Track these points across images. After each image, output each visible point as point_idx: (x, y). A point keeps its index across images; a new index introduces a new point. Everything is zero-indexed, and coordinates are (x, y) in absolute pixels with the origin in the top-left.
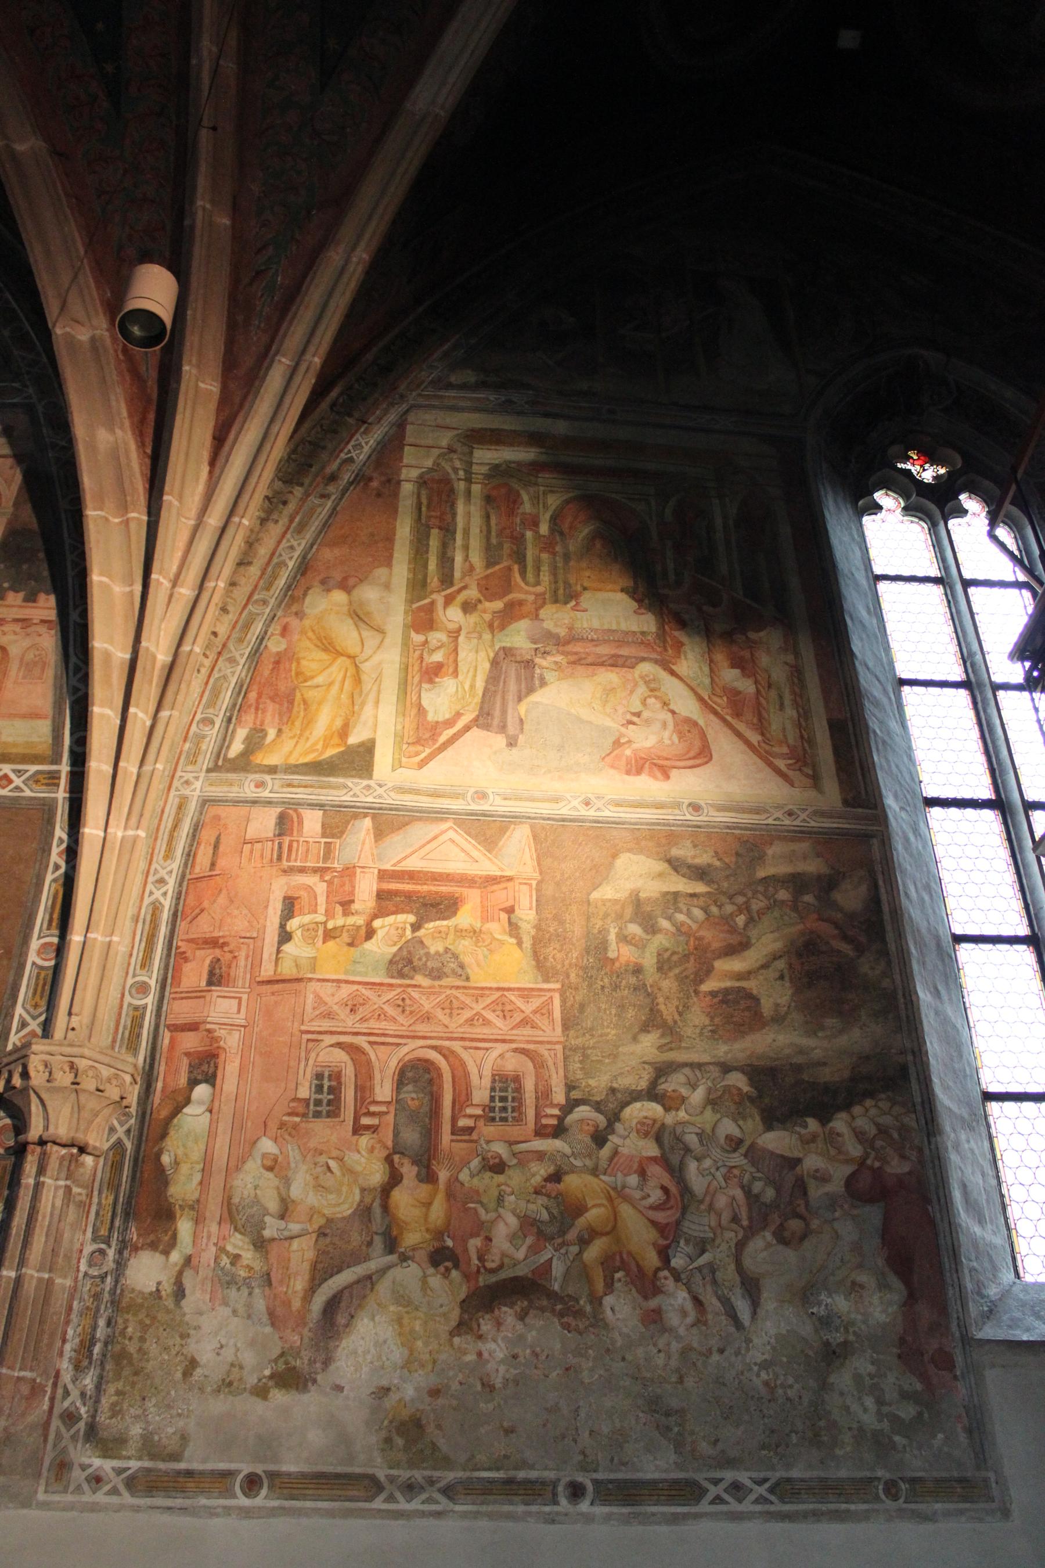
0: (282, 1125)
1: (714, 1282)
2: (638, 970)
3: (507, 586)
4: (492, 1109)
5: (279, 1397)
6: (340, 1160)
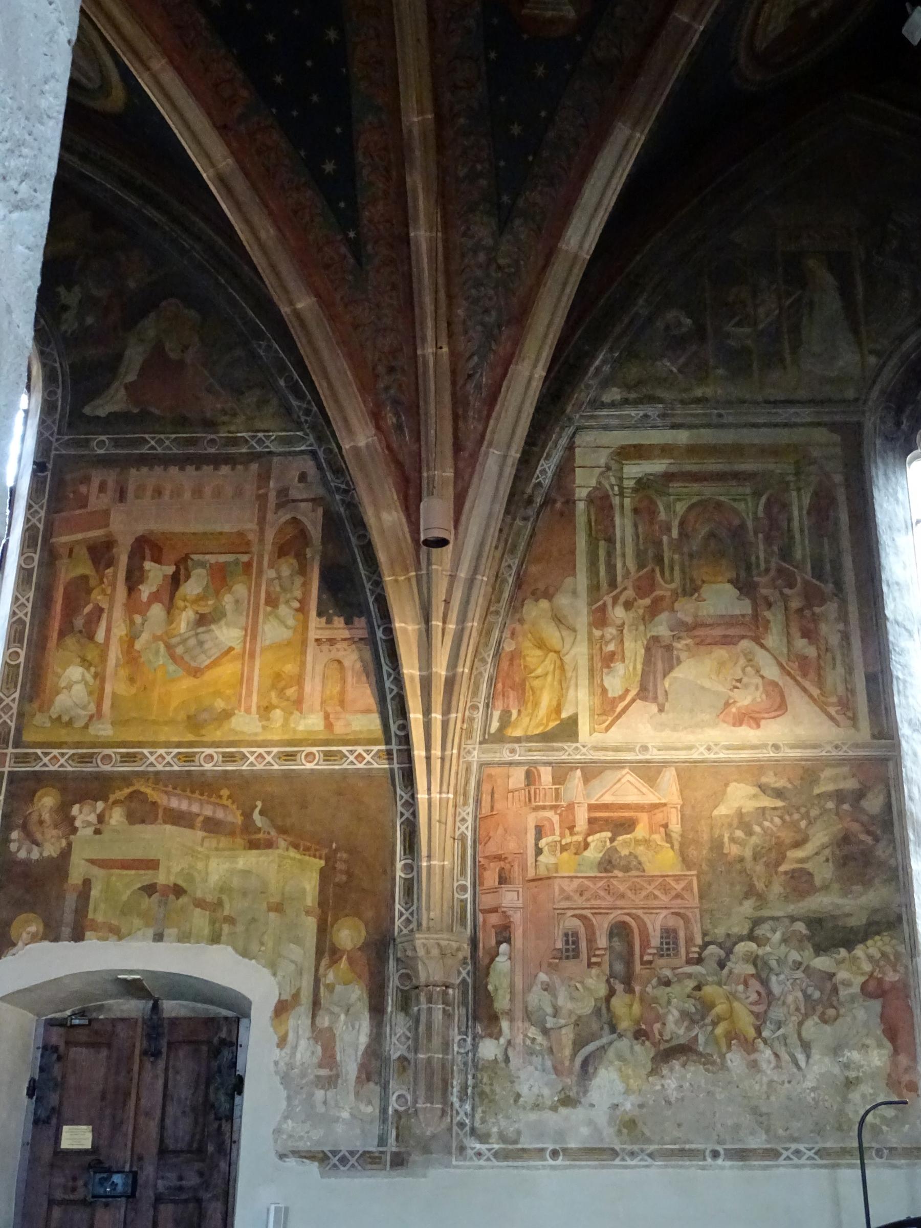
0: (550, 965)
1: (786, 1045)
2: (741, 860)
3: (652, 586)
4: (662, 949)
5: (563, 1111)
6: (582, 982)
